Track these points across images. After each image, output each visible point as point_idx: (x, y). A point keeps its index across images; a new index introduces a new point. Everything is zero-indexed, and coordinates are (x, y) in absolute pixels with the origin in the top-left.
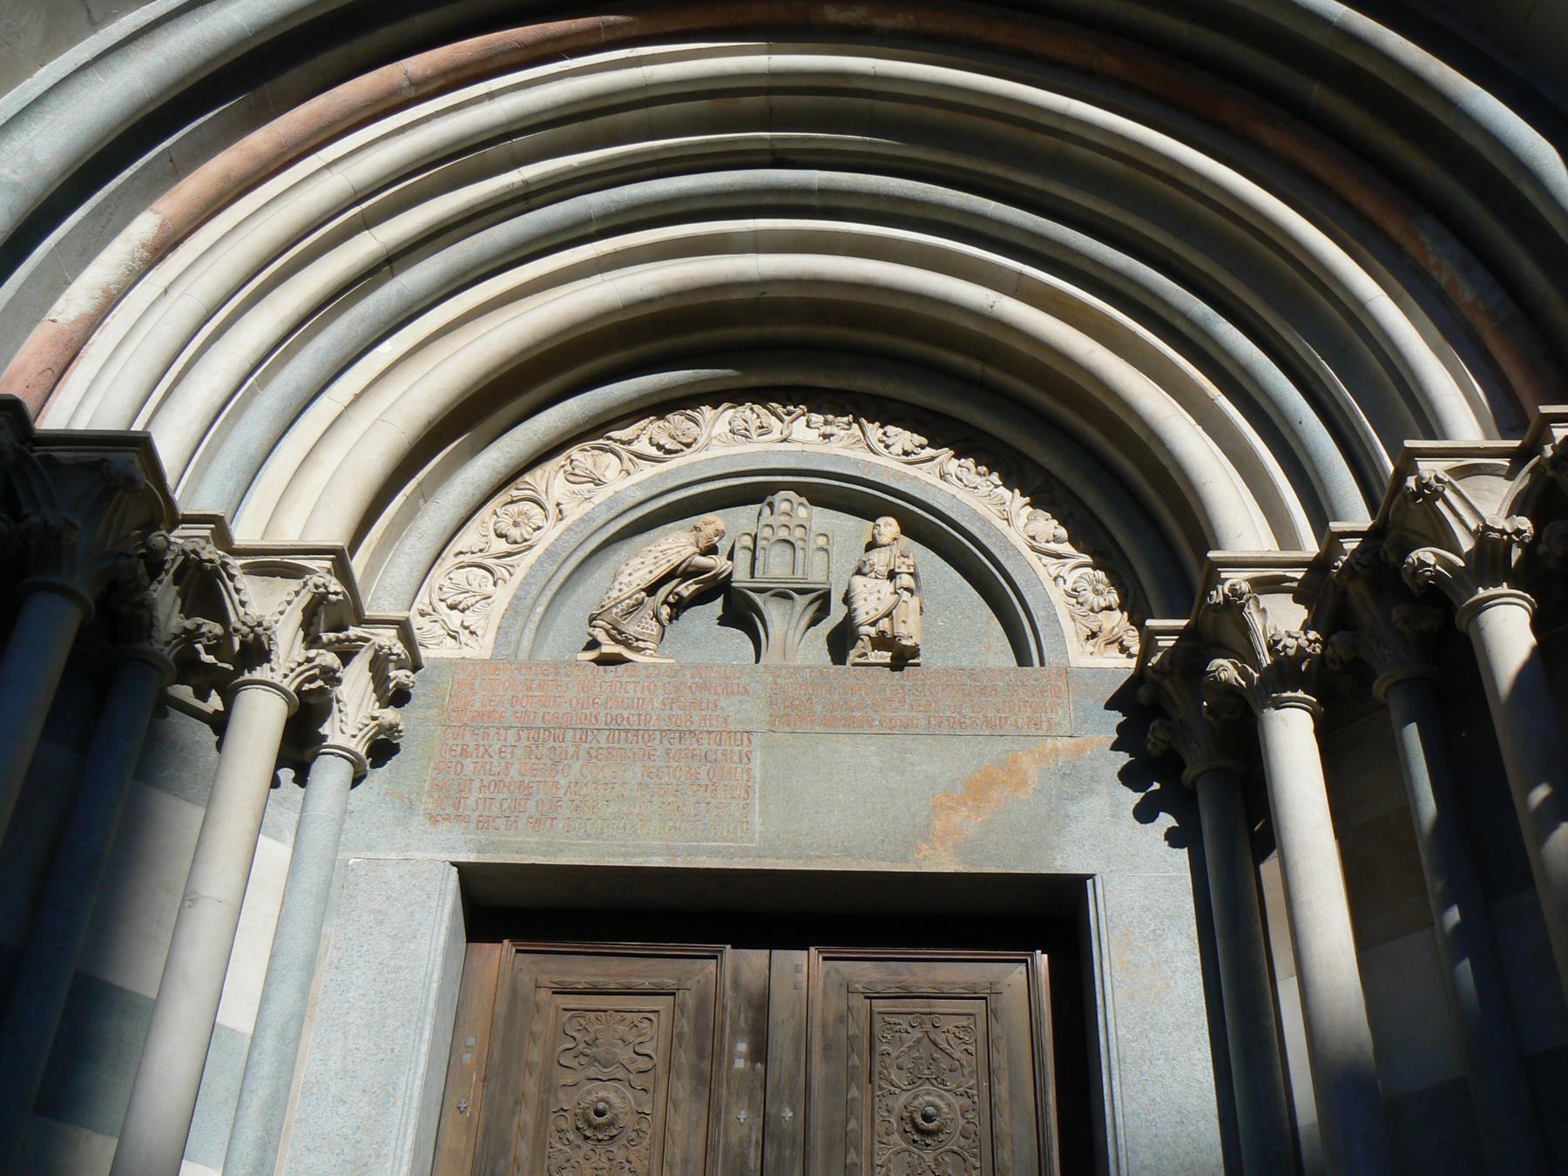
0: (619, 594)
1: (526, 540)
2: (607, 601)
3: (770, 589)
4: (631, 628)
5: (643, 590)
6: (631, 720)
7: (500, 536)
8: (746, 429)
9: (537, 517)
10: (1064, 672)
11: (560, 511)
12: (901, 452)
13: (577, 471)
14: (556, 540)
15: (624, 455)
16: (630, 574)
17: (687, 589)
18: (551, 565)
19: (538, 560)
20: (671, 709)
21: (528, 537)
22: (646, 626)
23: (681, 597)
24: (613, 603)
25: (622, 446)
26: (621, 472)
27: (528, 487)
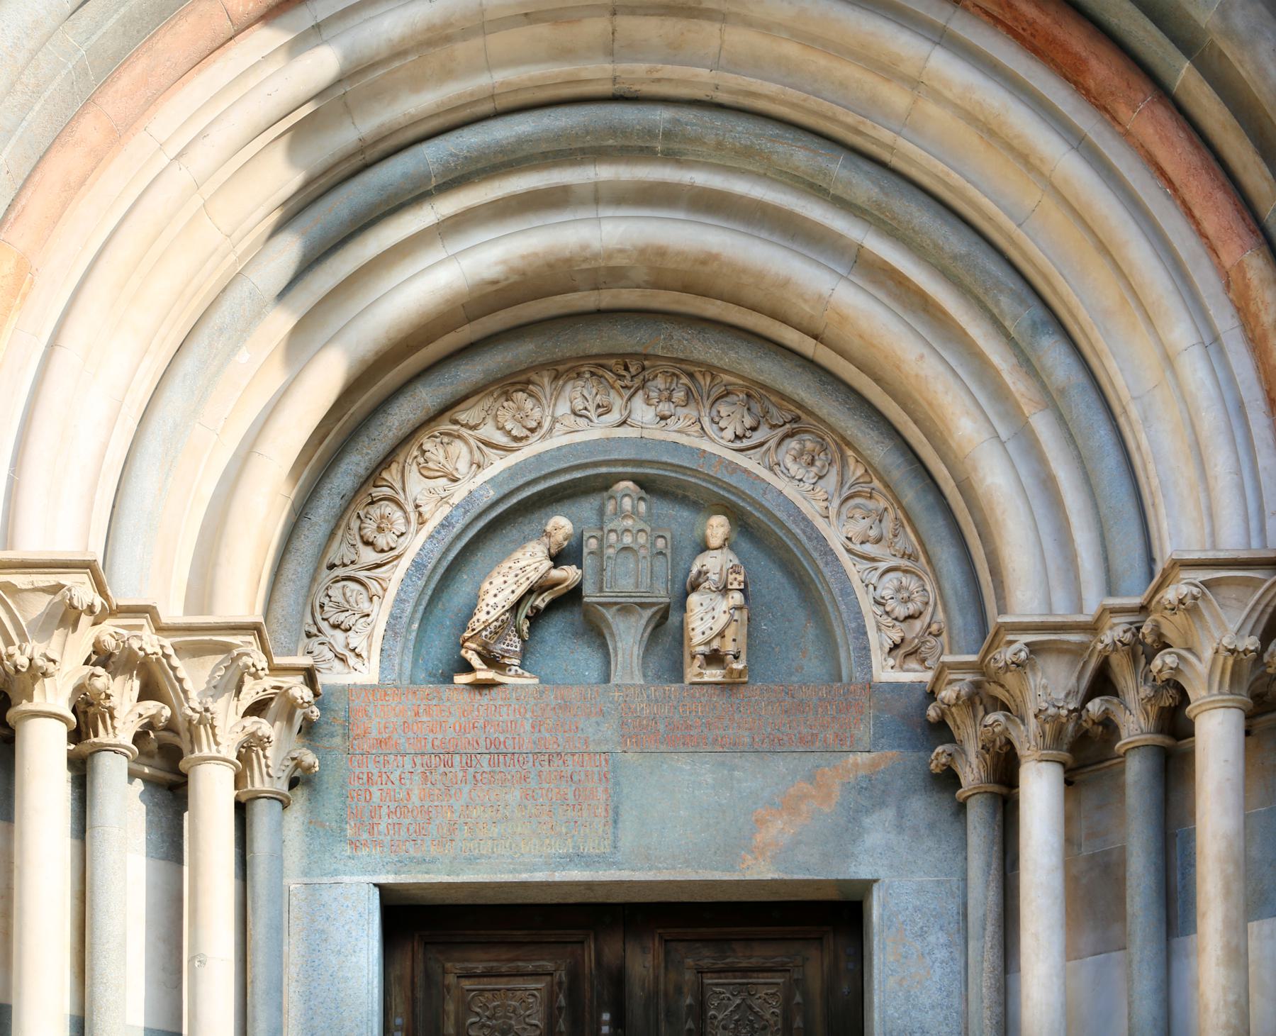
0: (488, 617)
1: (392, 549)
2: (477, 624)
3: (616, 604)
4: (498, 648)
5: (507, 611)
6: (507, 744)
7: (367, 543)
8: (586, 409)
9: (399, 521)
10: (868, 686)
11: (420, 514)
12: (732, 437)
13: (431, 465)
14: (421, 550)
15: (472, 441)
16: (495, 596)
17: (541, 602)
18: (419, 579)
19: (407, 574)
20: (540, 731)
21: (393, 546)
22: (511, 643)
23: (537, 608)
24: (483, 627)
25: (470, 432)
26: (471, 465)
27: (385, 483)
